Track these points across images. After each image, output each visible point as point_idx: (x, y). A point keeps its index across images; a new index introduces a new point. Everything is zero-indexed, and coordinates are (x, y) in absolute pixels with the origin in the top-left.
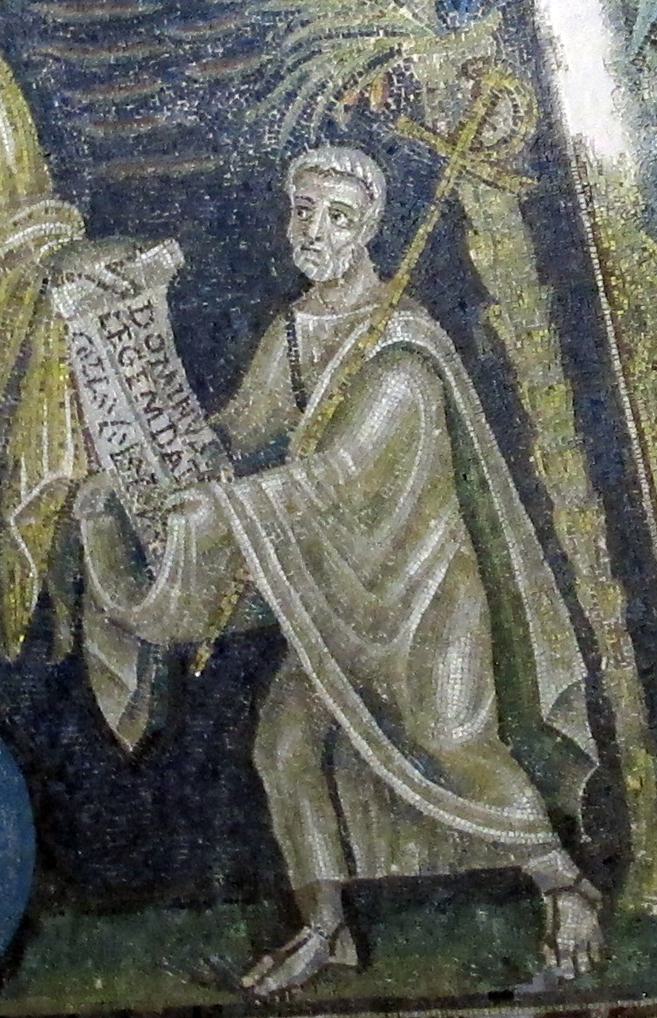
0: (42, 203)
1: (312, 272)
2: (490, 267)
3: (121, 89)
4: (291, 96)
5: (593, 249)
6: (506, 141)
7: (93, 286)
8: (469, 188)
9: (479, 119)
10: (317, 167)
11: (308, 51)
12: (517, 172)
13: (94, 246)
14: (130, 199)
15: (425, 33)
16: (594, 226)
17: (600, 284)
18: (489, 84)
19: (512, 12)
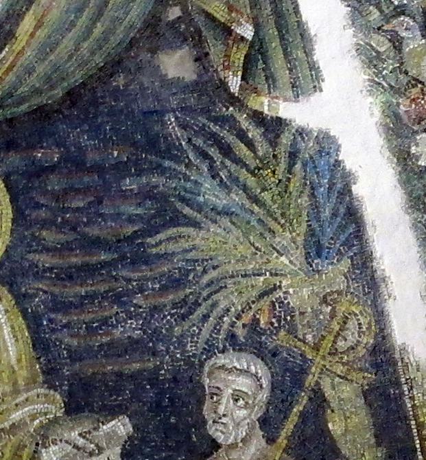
0: (35, 390)
1: (221, 438)
2: (343, 434)
3: (89, 312)
4: (205, 317)
5: (413, 422)
6: (353, 348)
7: (70, 447)
8: (328, 380)
9: (334, 333)
10: (223, 366)
11: (217, 286)
12: (361, 370)
13: (71, 420)
14: (96, 388)
15: (297, 274)
16: (414, 406)
17: (418, 446)
18: (342, 309)
19: (358, 260)
